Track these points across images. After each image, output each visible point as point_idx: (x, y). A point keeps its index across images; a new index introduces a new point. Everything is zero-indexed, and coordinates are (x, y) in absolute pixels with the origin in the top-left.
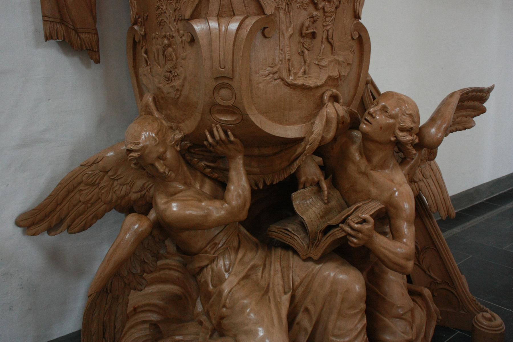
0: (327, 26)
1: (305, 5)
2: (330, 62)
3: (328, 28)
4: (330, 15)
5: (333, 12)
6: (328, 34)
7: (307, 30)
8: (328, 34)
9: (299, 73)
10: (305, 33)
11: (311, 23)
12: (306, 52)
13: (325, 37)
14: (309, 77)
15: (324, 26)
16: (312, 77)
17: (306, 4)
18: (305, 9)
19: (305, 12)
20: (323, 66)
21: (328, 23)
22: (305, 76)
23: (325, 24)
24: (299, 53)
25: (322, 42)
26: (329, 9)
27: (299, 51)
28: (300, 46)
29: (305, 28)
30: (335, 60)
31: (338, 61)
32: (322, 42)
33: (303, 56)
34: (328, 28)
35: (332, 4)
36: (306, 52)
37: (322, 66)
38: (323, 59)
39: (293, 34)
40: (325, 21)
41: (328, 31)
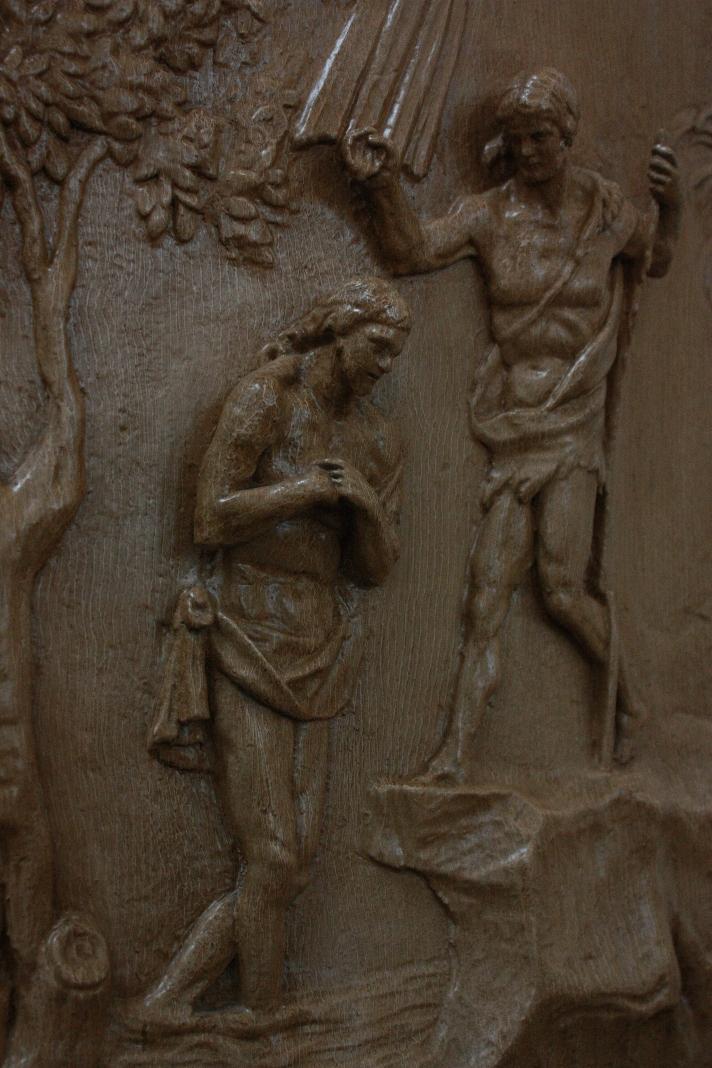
0: (527, 444)
1: (244, 205)
2: (557, 844)
3: (535, 469)
4: (557, 332)
5: (585, 301)
6: (536, 537)
7: (260, 477)
8: (536, 537)
9: (154, 978)
10: (226, 515)
11: (302, 408)
12: (253, 730)
13: (499, 564)
14: (293, 1026)
15: (491, 451)
16: (332, 1024)
17: (255, 192)
18: (249, 256)
19: (242, 288)
20: (491, 893)
21: (529, 420)
22: (244, 1015)
23: (497, 429)
24: (161, 750)
25: (468, 617)
26: (540, 271)
27: (161, 727)
28: (178, 658)
29: (218, 459)
30: (630, 810)
31: (672, 823)
32: (468, 617)
33: (218, 777)
34: (535, 469)
35: (570, 213)
36: (253, 730)
37: (471, 888)
38: (484, 803)
39: (66, 518)
40: (507, 399)
41: (535, 502)
